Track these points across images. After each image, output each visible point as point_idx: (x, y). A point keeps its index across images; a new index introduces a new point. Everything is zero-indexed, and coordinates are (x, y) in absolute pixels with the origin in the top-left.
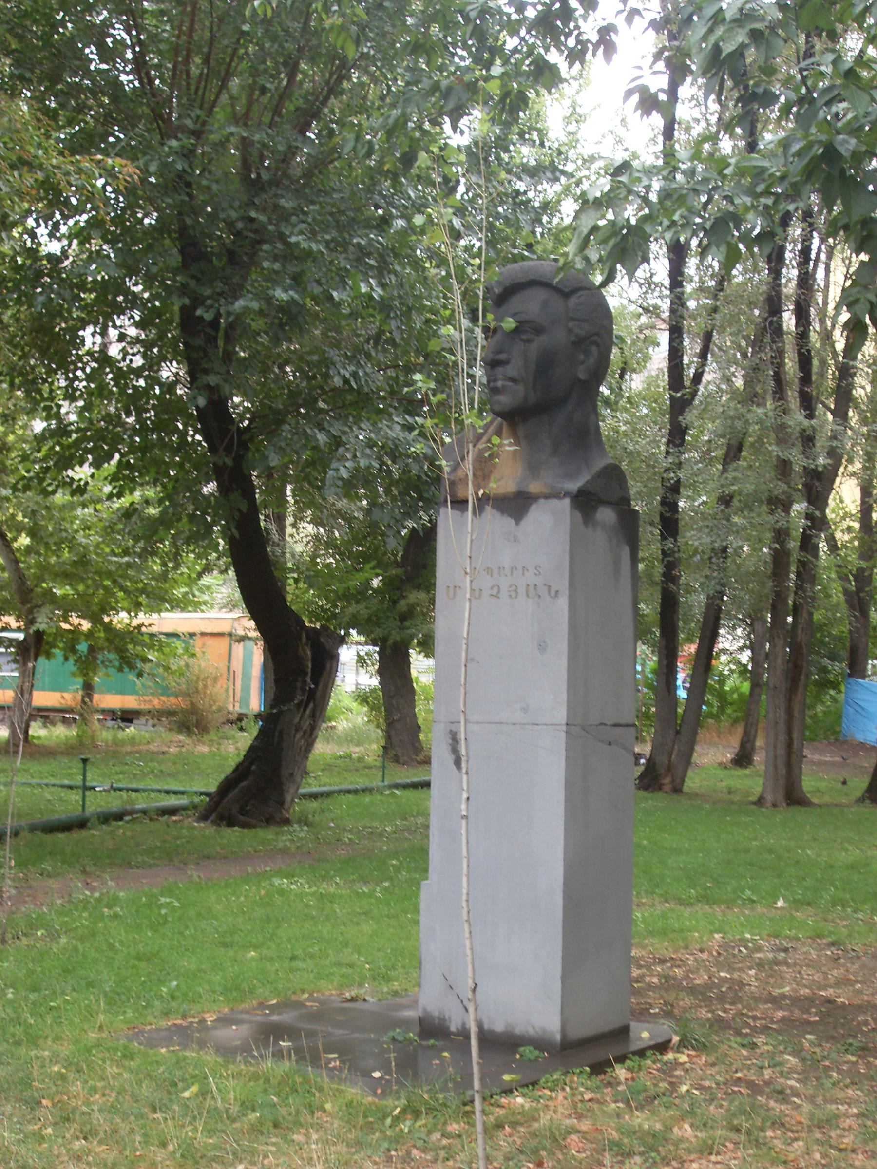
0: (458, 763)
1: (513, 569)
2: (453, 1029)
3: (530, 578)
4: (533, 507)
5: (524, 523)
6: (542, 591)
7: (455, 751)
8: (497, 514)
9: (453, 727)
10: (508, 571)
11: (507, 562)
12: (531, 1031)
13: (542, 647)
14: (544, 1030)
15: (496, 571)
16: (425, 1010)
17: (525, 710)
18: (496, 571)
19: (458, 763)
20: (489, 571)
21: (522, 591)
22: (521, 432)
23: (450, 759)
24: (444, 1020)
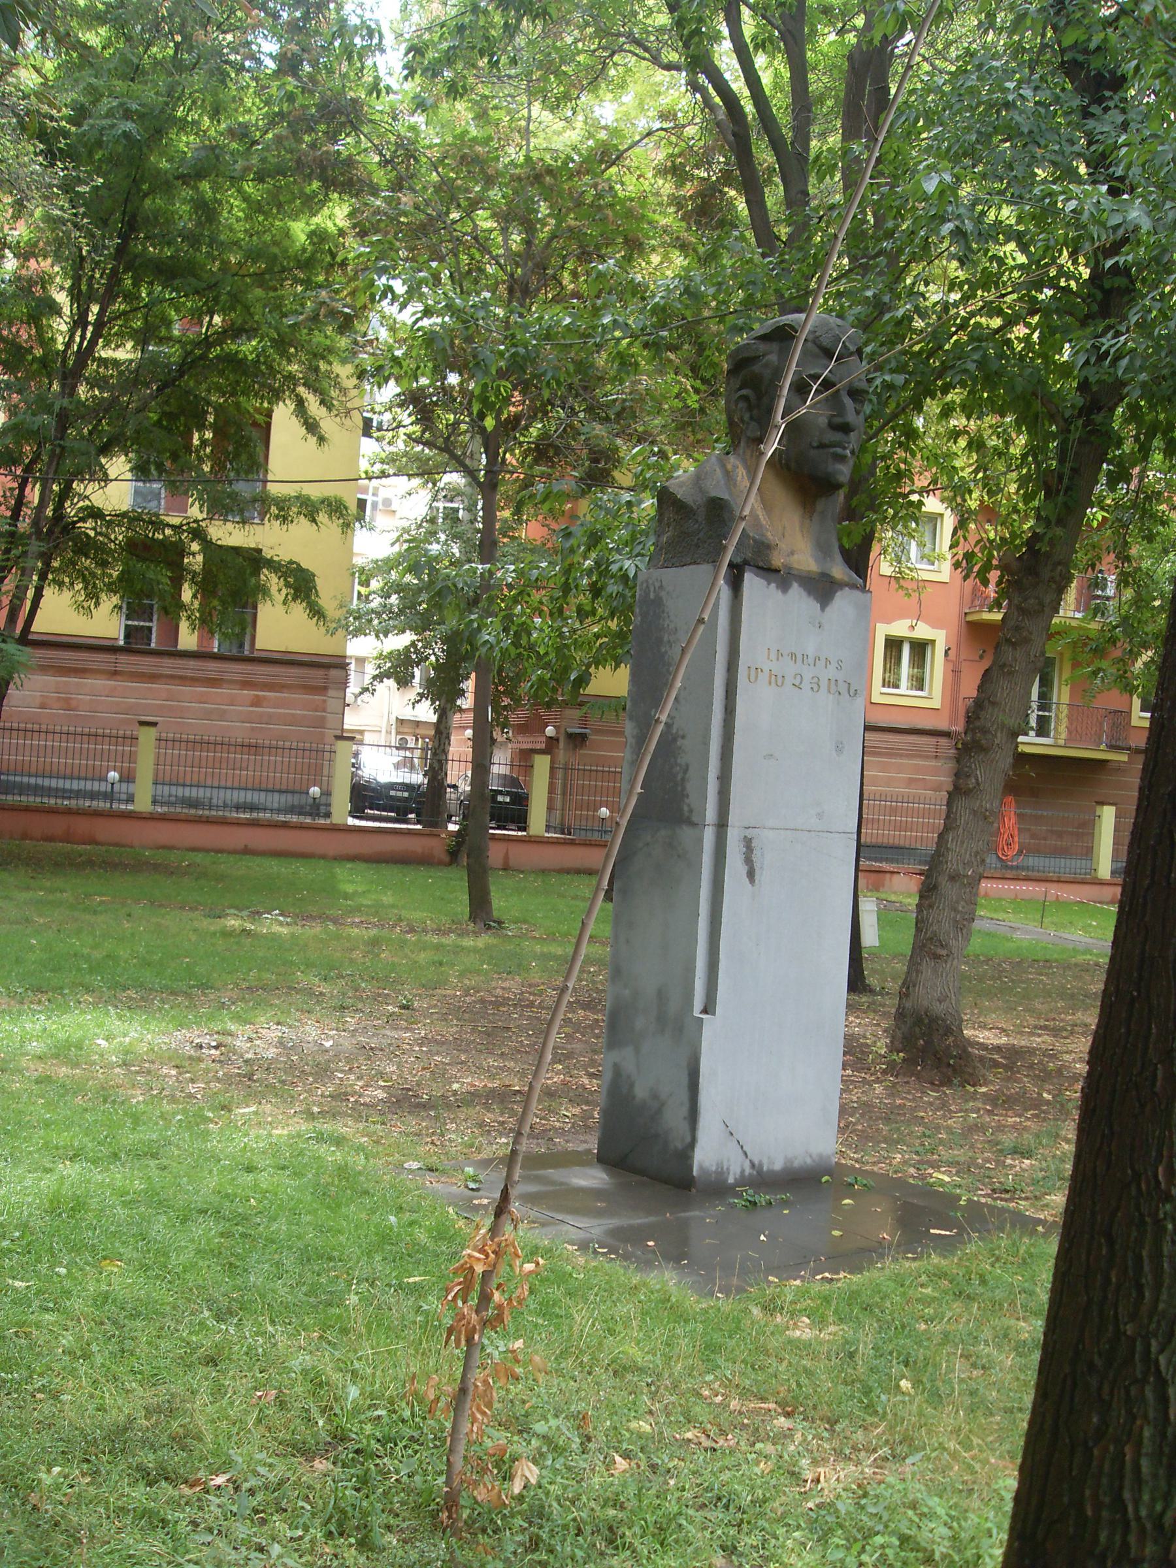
0: (751, 875)
1: (817, 659)
2: (731, 1180)
3: (831, 672)
4: (839, 594)
5: (828, 609)
6: (843, 688)
7: (749, 861)
8: (804, 594)
9: (749, 833)
10: (811, 661)
11: (811, 651)
12: (809, 1161)
13: (839, 748)
14: (821, 1156)
15: (799, 657)
16: (701, 1167)
17: (820, 816)
18: (799, 657)
19: (751, 875)
20: (793, 656)
21: (824, 684)
22: (821, 505)
23: (743, 870)
24: (722, 1173)
